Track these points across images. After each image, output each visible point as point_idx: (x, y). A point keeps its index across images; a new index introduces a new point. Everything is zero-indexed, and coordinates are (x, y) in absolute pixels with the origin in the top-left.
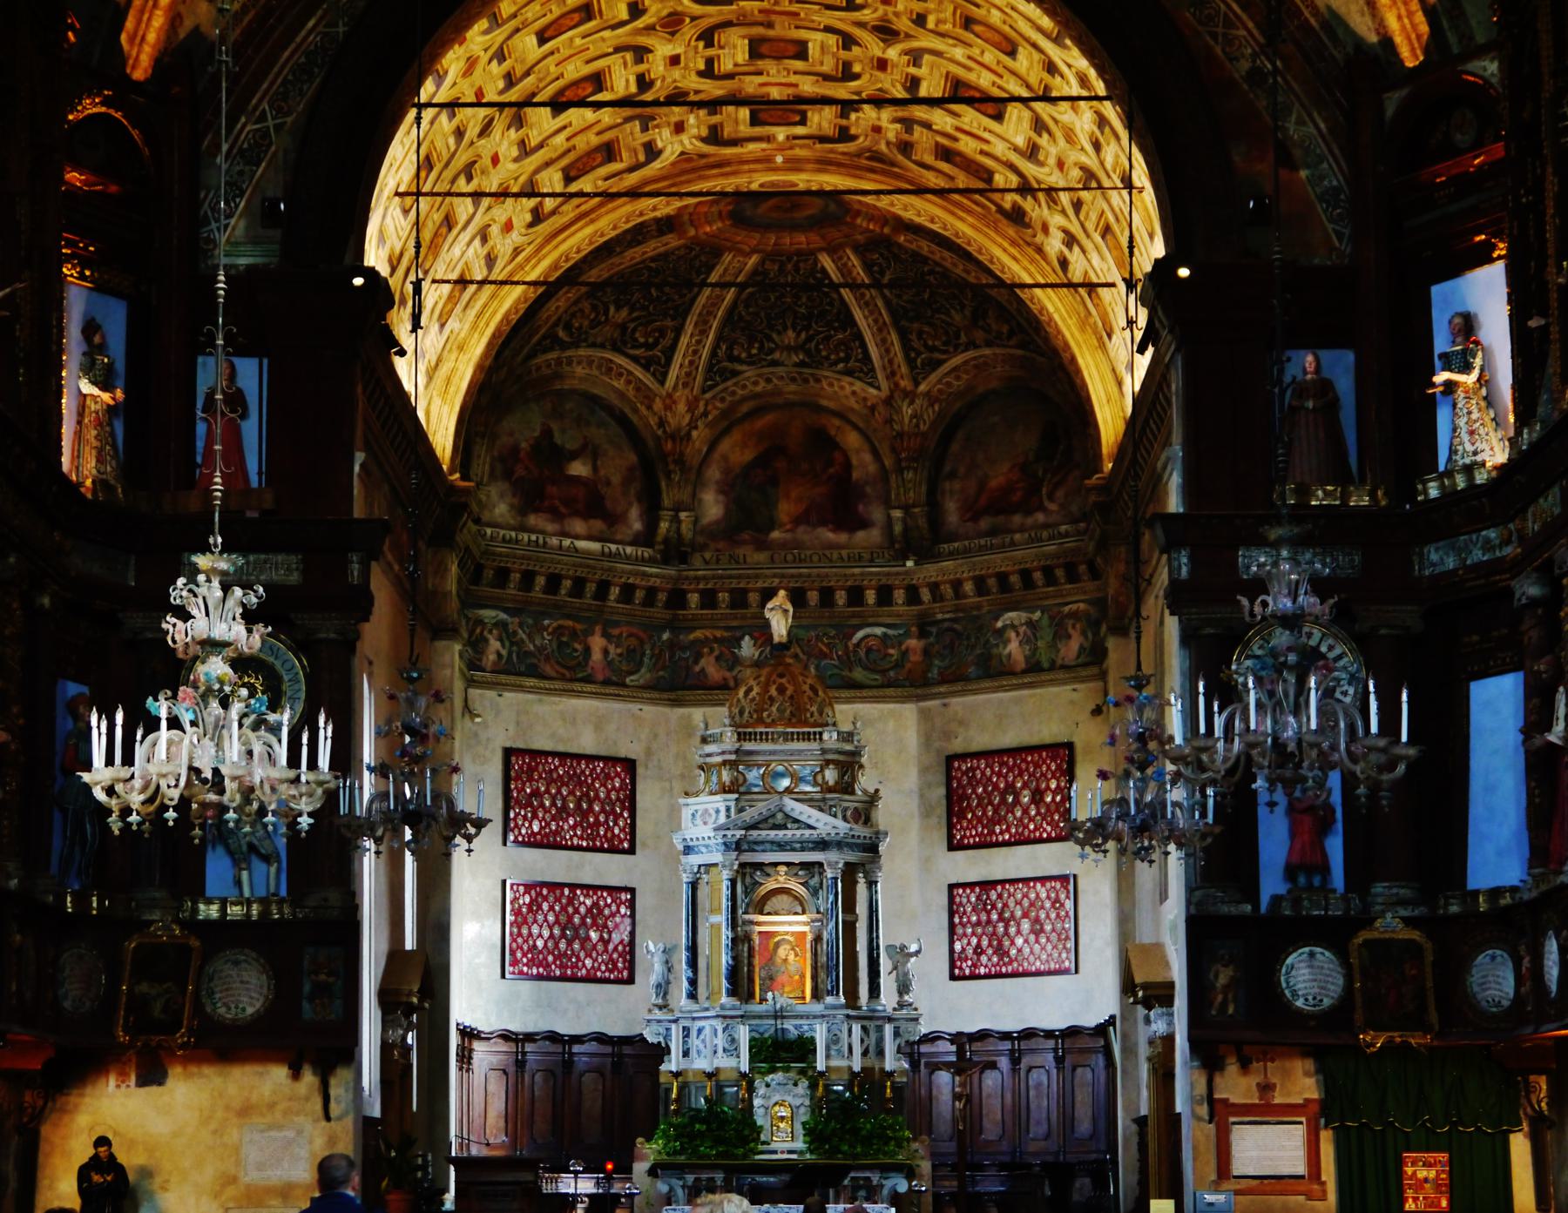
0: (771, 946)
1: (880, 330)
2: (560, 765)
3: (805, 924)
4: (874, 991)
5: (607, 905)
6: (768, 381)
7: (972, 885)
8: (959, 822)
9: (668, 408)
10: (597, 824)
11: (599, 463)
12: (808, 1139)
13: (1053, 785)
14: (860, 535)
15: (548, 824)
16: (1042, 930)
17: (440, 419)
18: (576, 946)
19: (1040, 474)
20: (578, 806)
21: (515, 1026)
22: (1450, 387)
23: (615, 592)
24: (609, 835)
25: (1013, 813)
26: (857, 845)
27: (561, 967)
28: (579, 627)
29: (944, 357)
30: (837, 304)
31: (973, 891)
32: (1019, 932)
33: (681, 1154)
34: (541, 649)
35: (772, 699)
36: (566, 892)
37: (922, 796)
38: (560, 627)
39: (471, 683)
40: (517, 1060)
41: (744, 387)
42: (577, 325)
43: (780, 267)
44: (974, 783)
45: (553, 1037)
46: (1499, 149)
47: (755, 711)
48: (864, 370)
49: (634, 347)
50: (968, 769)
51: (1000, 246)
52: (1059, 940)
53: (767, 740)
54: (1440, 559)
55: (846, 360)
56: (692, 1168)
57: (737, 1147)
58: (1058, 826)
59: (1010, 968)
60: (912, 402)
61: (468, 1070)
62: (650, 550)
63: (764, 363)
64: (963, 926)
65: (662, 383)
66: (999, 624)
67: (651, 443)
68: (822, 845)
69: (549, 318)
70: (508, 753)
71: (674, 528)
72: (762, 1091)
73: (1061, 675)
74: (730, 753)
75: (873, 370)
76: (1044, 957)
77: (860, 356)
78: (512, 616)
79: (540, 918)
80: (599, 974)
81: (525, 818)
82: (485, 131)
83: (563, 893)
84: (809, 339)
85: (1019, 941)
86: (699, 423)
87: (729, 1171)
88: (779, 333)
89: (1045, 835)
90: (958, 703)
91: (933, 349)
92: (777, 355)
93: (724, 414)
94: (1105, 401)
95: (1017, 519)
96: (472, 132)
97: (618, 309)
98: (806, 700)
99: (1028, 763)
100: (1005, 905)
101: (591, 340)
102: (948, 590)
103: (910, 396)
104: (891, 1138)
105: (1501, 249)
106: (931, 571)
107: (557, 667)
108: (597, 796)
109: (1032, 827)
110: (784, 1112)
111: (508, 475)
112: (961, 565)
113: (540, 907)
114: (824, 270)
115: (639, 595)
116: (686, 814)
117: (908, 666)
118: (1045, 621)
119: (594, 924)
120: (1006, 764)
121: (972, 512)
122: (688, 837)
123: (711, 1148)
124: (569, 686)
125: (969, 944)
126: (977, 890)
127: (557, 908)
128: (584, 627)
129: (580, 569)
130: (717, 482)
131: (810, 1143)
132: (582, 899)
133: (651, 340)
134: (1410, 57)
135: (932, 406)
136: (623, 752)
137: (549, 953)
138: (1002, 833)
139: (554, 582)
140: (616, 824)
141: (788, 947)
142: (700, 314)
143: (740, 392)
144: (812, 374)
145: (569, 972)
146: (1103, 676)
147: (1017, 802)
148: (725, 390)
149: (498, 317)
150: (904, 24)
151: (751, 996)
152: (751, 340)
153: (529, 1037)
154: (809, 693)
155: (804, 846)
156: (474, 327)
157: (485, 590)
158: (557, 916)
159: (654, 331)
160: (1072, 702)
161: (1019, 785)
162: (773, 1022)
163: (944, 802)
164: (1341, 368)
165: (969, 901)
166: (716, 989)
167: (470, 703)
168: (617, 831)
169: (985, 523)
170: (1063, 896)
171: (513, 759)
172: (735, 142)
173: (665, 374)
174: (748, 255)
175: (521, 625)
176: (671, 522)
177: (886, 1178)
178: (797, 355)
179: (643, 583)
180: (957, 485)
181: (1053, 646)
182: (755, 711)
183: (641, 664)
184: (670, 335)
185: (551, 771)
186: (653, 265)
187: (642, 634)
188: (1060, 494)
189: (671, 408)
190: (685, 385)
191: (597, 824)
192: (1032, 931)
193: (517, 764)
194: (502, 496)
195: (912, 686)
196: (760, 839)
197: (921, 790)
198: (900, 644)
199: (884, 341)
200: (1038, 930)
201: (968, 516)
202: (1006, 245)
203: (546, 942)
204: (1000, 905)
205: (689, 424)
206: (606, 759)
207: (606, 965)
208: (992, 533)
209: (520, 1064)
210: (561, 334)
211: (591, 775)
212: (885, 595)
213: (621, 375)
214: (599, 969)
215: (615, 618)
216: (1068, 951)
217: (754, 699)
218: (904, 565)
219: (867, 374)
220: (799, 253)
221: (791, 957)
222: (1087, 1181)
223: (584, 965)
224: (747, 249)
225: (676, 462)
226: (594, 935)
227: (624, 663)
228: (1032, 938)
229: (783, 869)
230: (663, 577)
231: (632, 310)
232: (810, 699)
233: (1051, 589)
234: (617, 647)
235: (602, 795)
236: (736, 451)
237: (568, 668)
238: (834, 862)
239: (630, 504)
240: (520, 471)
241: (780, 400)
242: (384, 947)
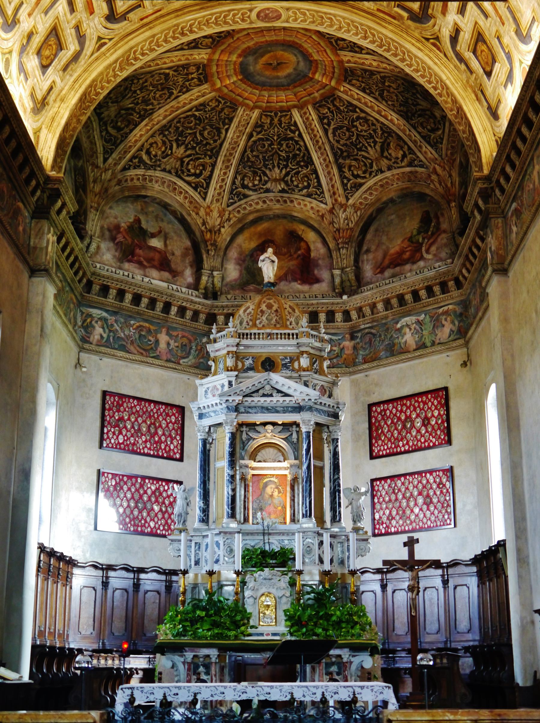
0: (261, 485)
1: (327, 166)
2: (138, 405)
3: (285, 469)
4: (336, 518)
5: (164, 490)
6: (264, 202)
7: (385, 479)
8: (376, 442)
9: (207, 214)
10: (160, 442)
11: (168, 242)
12: (289, 623)
13: (436, 413)
14: (316, 286)
15: (128, 439)
16: (431, 502)
17: (46, 141)
18: (145, 514)
19: (421, 240)
20: (149, 431)
21: (103, 560)
23: (174, 310)
24: (167, 449)
25: (410, 433)
26: (324, 412)
27: (134, 525)
28: (152, 328)
29: (363, 181)
30: (303, 149)
31: (386, 482)
32: (416, 504)
33: (184, 636)
34: (128, 337)
35: (262, 312)
36: (139, 480)
37: (353, 430)
38: (141, 326)
39: (82, 349)
40: (103, 582)
41: (251, 205)
42: (154, 153)
43: (271, 121)
44: (384, 418)
45: (127, 569)
47: (251, 320)
49: (188, 175)
50: (381, 411)
51: (410, 42)
52: (443, 507)
53: (259, 338)
55: (308, 187)
57: (230, 630)
58: (440, 438)
59: (411, 527)
60: (345, 211)
61: (65, 585)
62: (196, 292)
63: (262, 191)
64: (381, 504)
65: (204, 199)
66: (399, 326)
67: (198, 234)
68: (299, 409)
69: (136, 141)
70: (105, 394)
71: (210, 281)
72: (251, 584)
73: (439, 348)
74: (233, 346)
75: (323, 192)
76: (433, 518)
77: (316, 184)
78: (111, 315)
79: (122, 495)
80: (159, 531)
81: (114, 433)
83: (137, 481)
84: (287, 174)
85: (416, 510)
86: (225, 225)
87: (222, 649)
88: (270, 170)
89: (431, 444)
90: (374, 373)
91: (357, 176)
92: (269, 185)
93: (240, 220)
94: (482, 130)
95: (408, 267)
97: (178, 146)
98: (287, 313)
99: (419, 403)
100: (407, 488)
101: (163, 166)
102: (367, 310)
103: (344, 207)
104: (356, 623)
106: (357, 300)
107: (138, 348)
108: (160, 426)
109: (423, 440)
110: (269, 602)
111: (113, 239)
112: (375, 294)
113: (122, 488)
114: (295, 124)
115: (189, 314)
116: (201, 391)
117: (344, 356)
118: (428, 319)
119: (157, 501)
120: (406, 405)
121: (380, 269)
122: (201, 406)
123: (209, 630)
124: (145, 359)
125: (384, 514)
126: (389, 481)
127: (133, 490)
128: (155, 328)
129: (153, 293)
130: (235, 259)
131: (292, 626)
132: (149, 486)
133: (198, 171)
135: (356, 212)
136: (177, 403)
137: (127, 516)
138: (403, 446)
139: (137, 299)
140: (172, 443)
141: (273, 486)
142: (225, 156)
143: (248, 208)
144: (289, 198)
145: (139, 529)
146: (467, 344)
147: (413, 426)
148: (241, 205)
149: (88, 82)
151: (246, 520)
152: (255, 173)
153: (110, 568)
154: (289, 309)
155: (286, 410)
156: (72, 87)
157: (93, 297)
158: (133, 494)
159: (199, 165)
160: (447, 364)
161: (414, 416)
162: (262, 538)
163: (367, 432)
165: (383, 488)
166: (220, 516)
167: (80, 361)
168: (172, 447)
169: (387, 273)
170: (444, 480)
171: (108, 398)
173: (206, 194)
174: (252, 109)
175: (116, 321)
176: (209, 277)
177: (354, 656)
178: (280, 185)
179: (191, 307)
180: (371, 256)
181: (433, 332)
182: (251, 320)
183: (189, 353)
184: (209, 169)
185: (132, 407)
186: (197, 113)
187: (190, 337)
188: (433, 249)
189: (209, 215)
190: (218, 200)
191: (160, 442)
192: (425, 503)
194: (108, 249)
195: (346, 367)
196: (253, 404)
197: (353, 426)
198: (340, 344)
199: (329, 173)
200: (428, 502)
201: (378, 271)
202: (414, 42)
203: (125, 510)
204: (403, 490)
205: (219, 225)
206: (167, 405)
207: (164, 526)
208: (393, 276)
209: (105, 584)
210: (145, 157)
211: (157, 412)
213: (181, 193)
214: (159, 528)
215: (175, 325)
216: (449, 514)
217: (250, 313)
218: (341, 298)
219: (319, 196)
220: (282, 110)
221: (276, 494)
222: (471, 659)
223: (149, 525)
224: (251, 104)
225: (211, 244)
226: (156, 508)
227: (179, 351)
228: (425, 507)
229: (269, 427)
230: (203, 305)
231: (187, 149)
232: (289, 313)
233: (431, 299)
234: (175, 342)
235: (164, 426)
237: (144, 350)
239: (186, 267)
240: (120, 238)
241: (271, 213)
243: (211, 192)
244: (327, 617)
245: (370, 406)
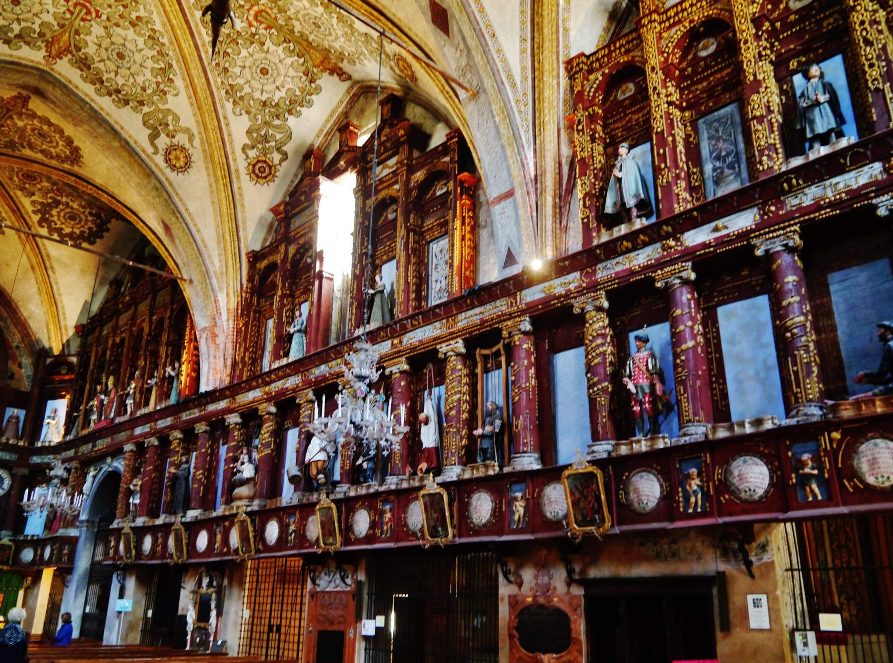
22: (49, 423)
46: (73, 376)
54: (36, 459)
105: (68, 396)
134: (56, 352)
164: (21, 413)
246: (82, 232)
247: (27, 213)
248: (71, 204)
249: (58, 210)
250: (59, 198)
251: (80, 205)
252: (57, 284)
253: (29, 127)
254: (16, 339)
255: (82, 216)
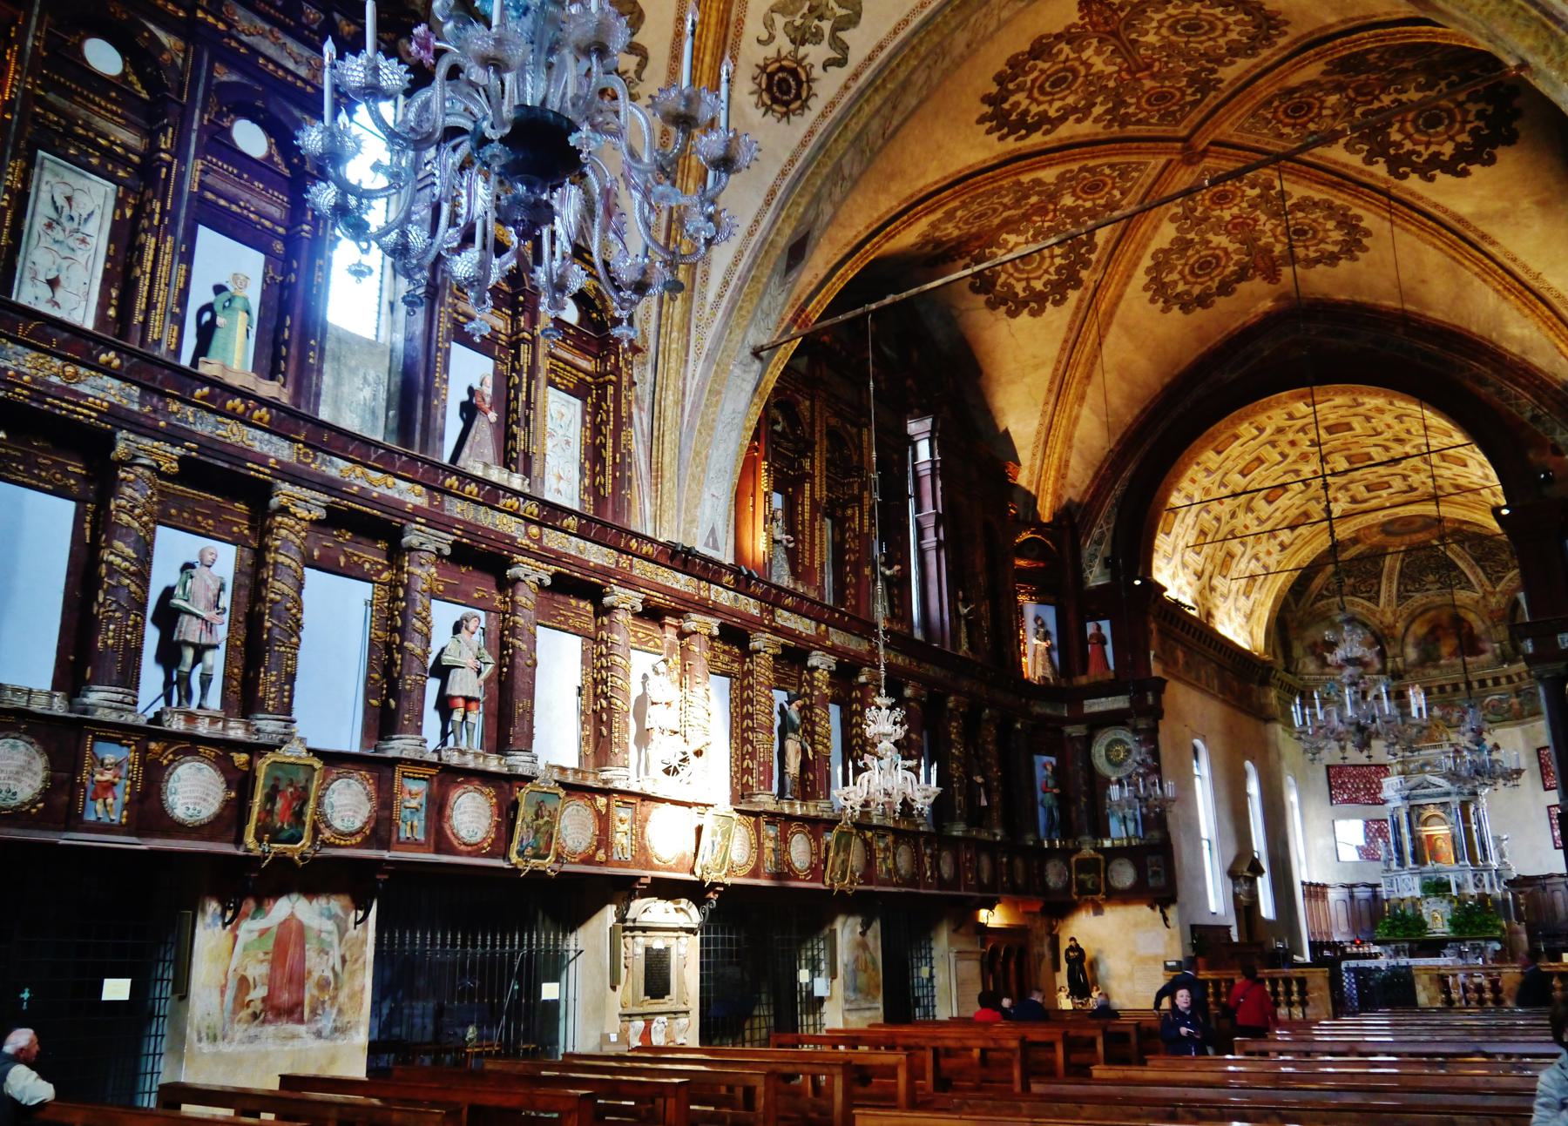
14: (1482, 657)
48: (1469, 586)
56: (1394, 942)
70: (1328, 767)
82: (1233, 515)
96: (1225, 517)
103: (1493, 594)
150: (1404, 436)
155: (1439, 795)
172: (1365, 501)
193: (1332, 772)
212: (1496, 681)
236: (1419, 629)
238: (1455, 800)
242: (1232, 852)
243: (1382, 601)
244: (1473, 922)
245: (1539, 750)
246: (1474, 133)
247: (1361, 172)
248: (1404, 97)
249: (1396, 126)
250: (1376, 105)
251: (1419, 88)
252: (1514, 260)
253: (1164, 31)
254: (1526, 406)
255: (1443, 103)
